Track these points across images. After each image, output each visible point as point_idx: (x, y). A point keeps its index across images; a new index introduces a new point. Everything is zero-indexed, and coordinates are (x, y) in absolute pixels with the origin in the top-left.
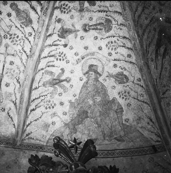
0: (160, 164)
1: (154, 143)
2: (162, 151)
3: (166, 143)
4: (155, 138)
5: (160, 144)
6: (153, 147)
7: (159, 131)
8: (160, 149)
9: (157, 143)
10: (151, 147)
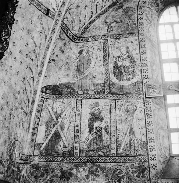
0: (43, 24)
1: (51, 9)
2: (51, 18)
3: (58, 14)
4: (54, 6)
5: (53, 12)
6: (48, 10)
7: (60, 5)
8: (51, 15)
9: (53, 10)
10: (47, 9)
